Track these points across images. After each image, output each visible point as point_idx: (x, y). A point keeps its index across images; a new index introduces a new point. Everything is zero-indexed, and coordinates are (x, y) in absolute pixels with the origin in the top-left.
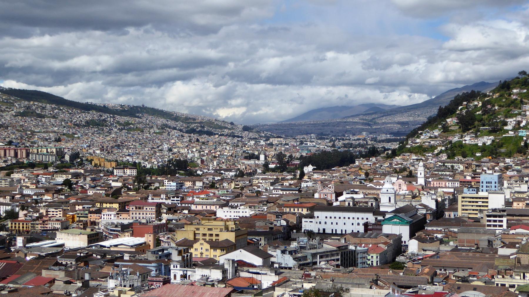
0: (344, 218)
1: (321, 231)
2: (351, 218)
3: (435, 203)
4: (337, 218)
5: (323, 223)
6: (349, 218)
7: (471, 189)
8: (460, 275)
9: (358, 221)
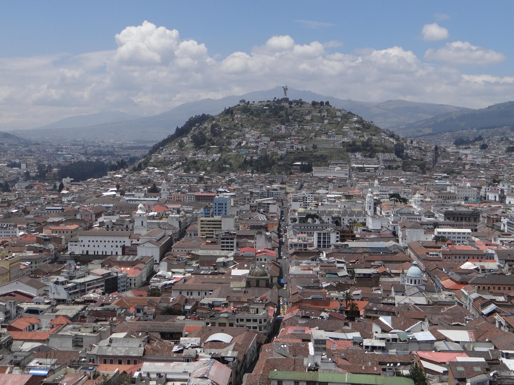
0: (105, 241)
1: (85, 253)
3: (178, 224)
4: (99, 241)
5: (86, 246)
6: (109, 241)
7: (206, 210)
8: (205, 303)
9: (116, 244)
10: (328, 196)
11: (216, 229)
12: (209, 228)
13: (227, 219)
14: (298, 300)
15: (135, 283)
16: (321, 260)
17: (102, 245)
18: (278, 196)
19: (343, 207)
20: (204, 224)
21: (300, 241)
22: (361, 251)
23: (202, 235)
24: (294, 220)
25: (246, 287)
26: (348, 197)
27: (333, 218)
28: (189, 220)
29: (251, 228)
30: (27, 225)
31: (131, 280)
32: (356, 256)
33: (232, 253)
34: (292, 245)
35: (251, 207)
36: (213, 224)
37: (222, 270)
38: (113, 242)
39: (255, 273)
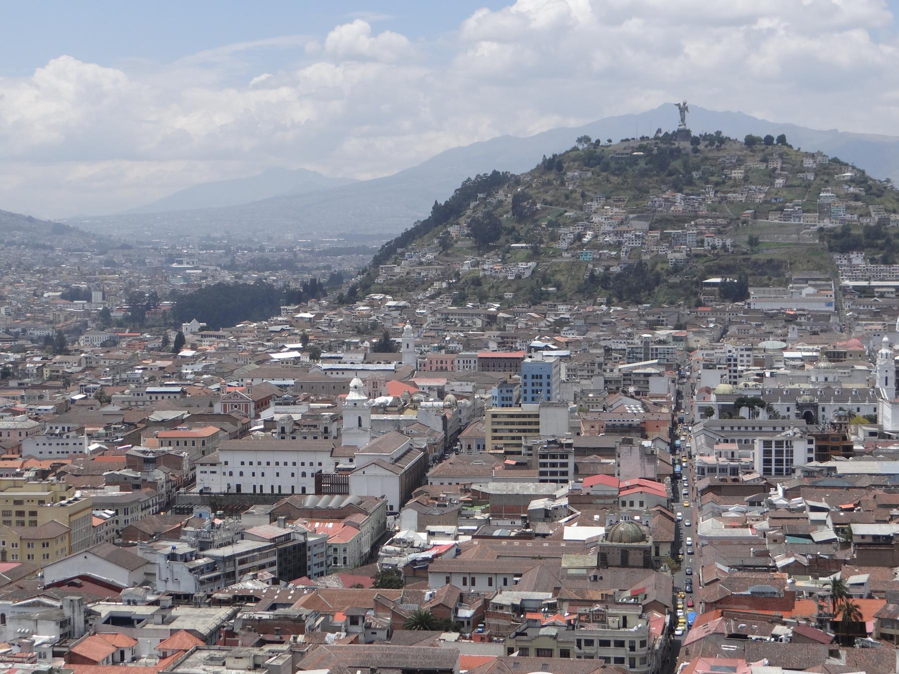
0: (277, 464)
2: (290, 464)
3: (441, 422)
4: (264, 464)
5: (236, 474)
6: (286, 464)
8: (504, 602)
9: (303, 469)
10: (787, 354)
11: (528, 434)
12: (511, 431)
13: (551, 411)
14: (718, 598)
15: (345, 558)
16: (772, 505)
17: (270, 471)
18: (669, 357)
19: (821, 379)
20: (499, 423)
21: (723, 461)
22: (866, 482)
23: (496, 448)
24: (708, 412)
25: (598, 567)
26: (835, 357)
27: (799, 406)
28: (464, 413)
29: (606, 431)
30: (106, 428)
31: (335, 550)
32: (855, 495)
33: (565, 489)
34: (703, 469)
35: (606, 382)
36: (520, 423)
37: (541, 527)
38: (294, 464)
39: (617, 536)
